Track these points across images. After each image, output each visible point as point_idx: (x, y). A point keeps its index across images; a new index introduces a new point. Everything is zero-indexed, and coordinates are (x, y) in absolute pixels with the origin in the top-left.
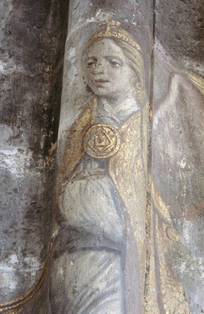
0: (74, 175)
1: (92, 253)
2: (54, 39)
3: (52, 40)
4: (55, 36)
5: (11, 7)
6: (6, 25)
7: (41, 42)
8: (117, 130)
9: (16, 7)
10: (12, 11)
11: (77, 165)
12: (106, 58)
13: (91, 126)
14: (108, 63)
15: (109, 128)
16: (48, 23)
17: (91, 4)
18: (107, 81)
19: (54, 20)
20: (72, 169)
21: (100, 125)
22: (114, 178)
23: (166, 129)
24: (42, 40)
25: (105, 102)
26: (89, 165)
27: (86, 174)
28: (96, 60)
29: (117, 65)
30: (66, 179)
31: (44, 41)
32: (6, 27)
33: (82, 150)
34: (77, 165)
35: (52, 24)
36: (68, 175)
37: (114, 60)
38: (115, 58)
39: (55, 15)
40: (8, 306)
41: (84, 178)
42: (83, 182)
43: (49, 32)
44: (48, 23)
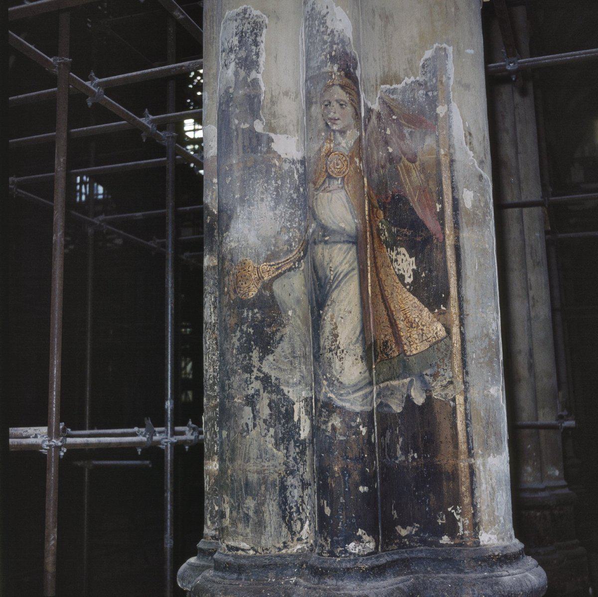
0: (323, 188)
1: (339, 246)
8: (347, 155)
11: (324, 181)
12: (337, 101)
13: (331, 153)
14: (338, 105)
15: (342, 154)
18: (339, 119)
20: (320, 184)
21: (336, 153)
22: (348, 192)
23: (372, 141)
25: (338, 135)
26: (332, 183)
27: (331, 188)
28: (330, 103)
29: (344, 106)
30: (317, 190)
33: (327, 171)
34: (324, 181)
36: (318, 187)
37: (342, 103)
38: (342, 100)
40: (284, 262)
41: (330, 191)
42: (329, 194)
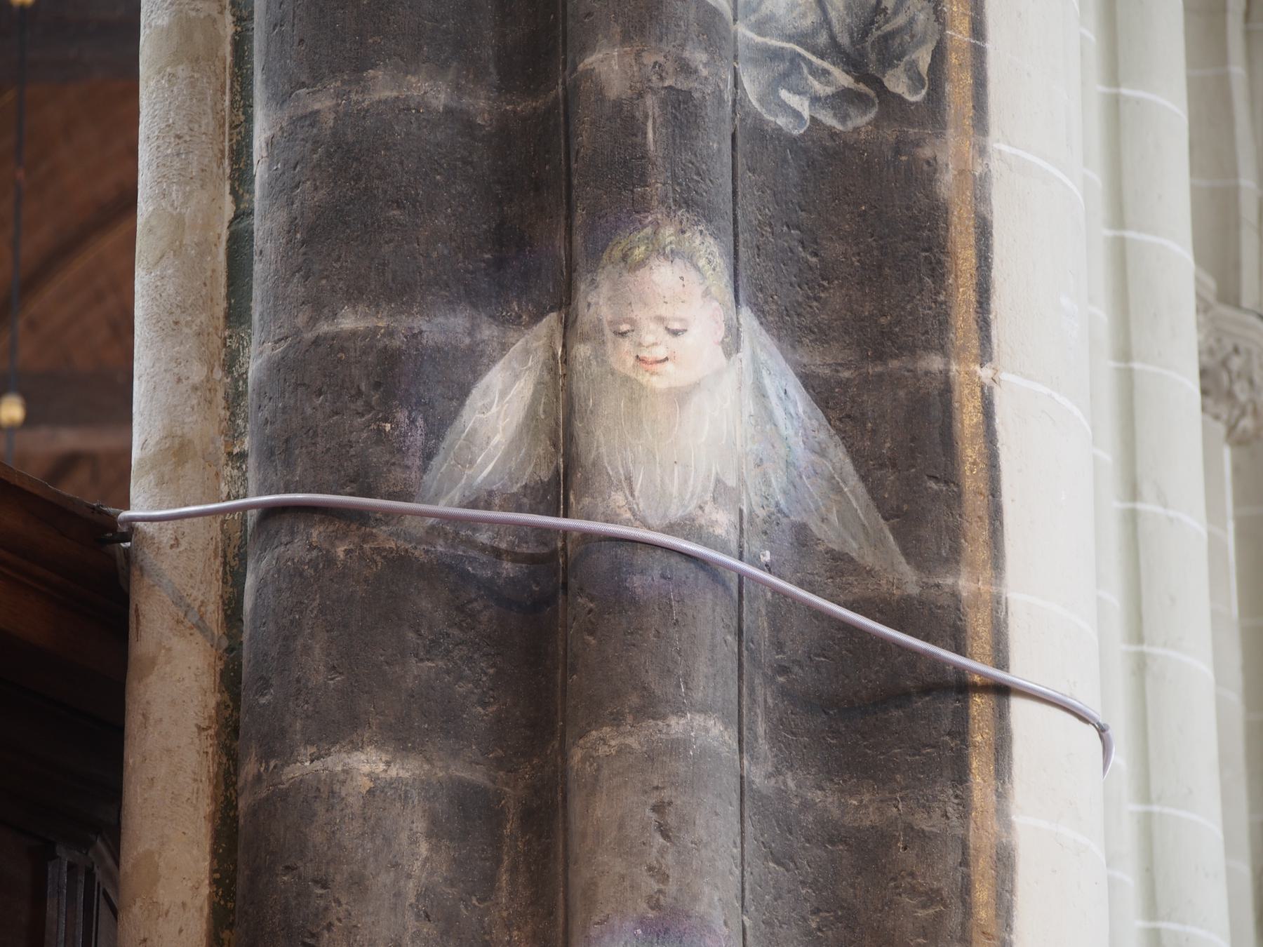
2: (515, 933)
3: (511, 937)
4: (519, 929)
5: (423, 848)
6: (418, 896)
7: (487, 938)
9: (434, 849)
10: (427, 859)
16: (500, 889)
17: (639, 931)
19: (512, 882)
24: (491, 932)
31: (493, 936)
32: (417, 900)
35: (511, 893)
39: (513, 870)
43: (505, 914)
44: (500, 889)
